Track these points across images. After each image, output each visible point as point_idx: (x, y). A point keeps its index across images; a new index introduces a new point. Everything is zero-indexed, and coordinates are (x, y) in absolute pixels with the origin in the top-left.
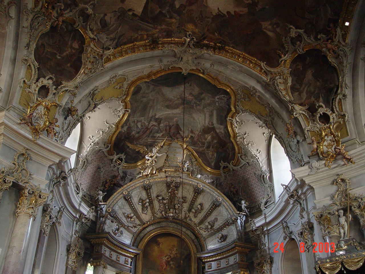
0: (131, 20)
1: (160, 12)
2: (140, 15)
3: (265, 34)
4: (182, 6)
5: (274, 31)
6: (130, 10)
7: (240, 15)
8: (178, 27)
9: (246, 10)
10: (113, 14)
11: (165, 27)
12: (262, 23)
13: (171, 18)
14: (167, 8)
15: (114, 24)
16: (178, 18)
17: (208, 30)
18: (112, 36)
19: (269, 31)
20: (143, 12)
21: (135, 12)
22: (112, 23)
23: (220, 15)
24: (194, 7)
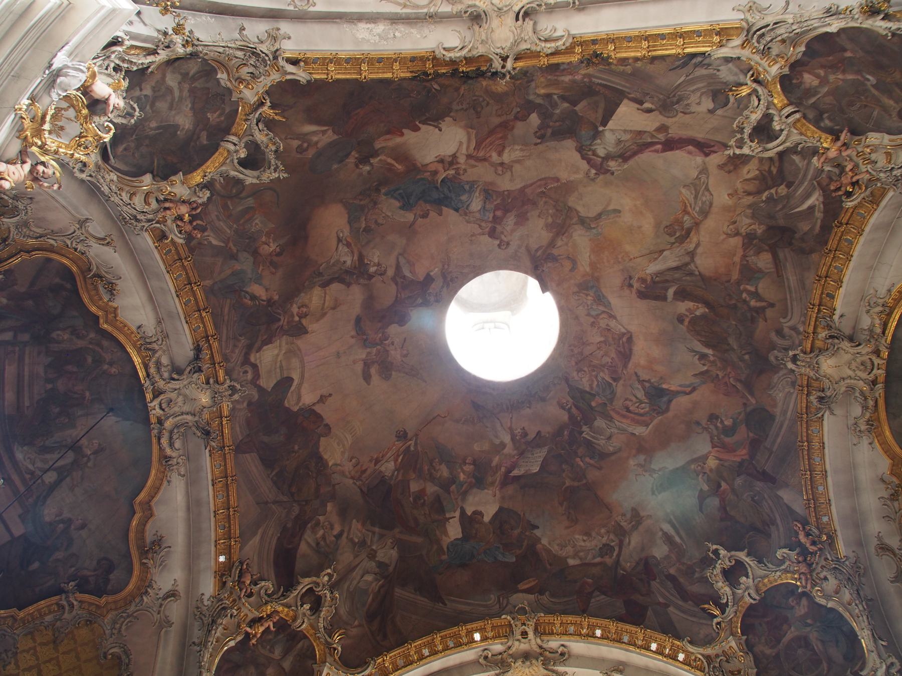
0: (648, 94)
1: (574, 103)
2: (625, 101)
3: (319, 123)
4: (524, 118)
5: (303, 137)
6: (649, 111)
7: (389, 132)
8: (532, 80)
9: (378, 145)
10: (692, 109)
11: (563, 78)
12: (336, 137)
13: (548, 96)
14: (558, 111)
15: (693, 91)
16: (531, 97)
17: (457, 89)
18: (702, 72)
19: (314, 133)
20: (618, 105)
21: (638, 106)
22: (699, 94)
23: (435, 120)
24: (496, 121)
